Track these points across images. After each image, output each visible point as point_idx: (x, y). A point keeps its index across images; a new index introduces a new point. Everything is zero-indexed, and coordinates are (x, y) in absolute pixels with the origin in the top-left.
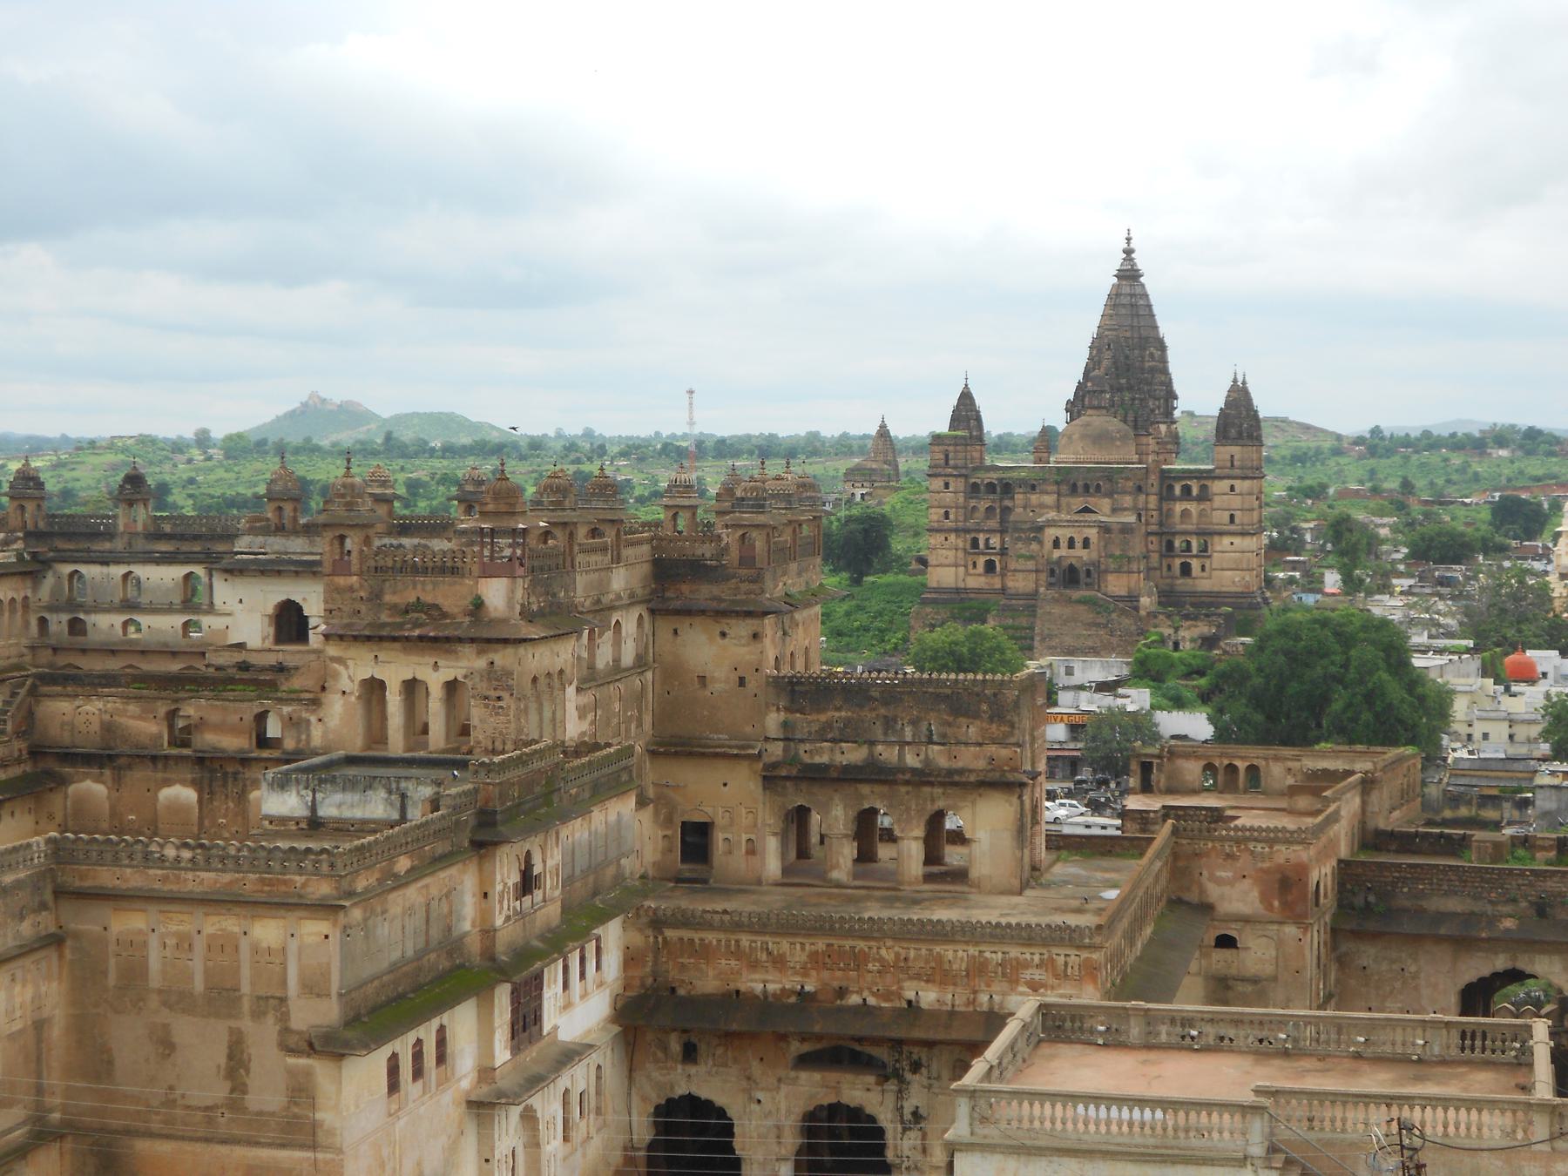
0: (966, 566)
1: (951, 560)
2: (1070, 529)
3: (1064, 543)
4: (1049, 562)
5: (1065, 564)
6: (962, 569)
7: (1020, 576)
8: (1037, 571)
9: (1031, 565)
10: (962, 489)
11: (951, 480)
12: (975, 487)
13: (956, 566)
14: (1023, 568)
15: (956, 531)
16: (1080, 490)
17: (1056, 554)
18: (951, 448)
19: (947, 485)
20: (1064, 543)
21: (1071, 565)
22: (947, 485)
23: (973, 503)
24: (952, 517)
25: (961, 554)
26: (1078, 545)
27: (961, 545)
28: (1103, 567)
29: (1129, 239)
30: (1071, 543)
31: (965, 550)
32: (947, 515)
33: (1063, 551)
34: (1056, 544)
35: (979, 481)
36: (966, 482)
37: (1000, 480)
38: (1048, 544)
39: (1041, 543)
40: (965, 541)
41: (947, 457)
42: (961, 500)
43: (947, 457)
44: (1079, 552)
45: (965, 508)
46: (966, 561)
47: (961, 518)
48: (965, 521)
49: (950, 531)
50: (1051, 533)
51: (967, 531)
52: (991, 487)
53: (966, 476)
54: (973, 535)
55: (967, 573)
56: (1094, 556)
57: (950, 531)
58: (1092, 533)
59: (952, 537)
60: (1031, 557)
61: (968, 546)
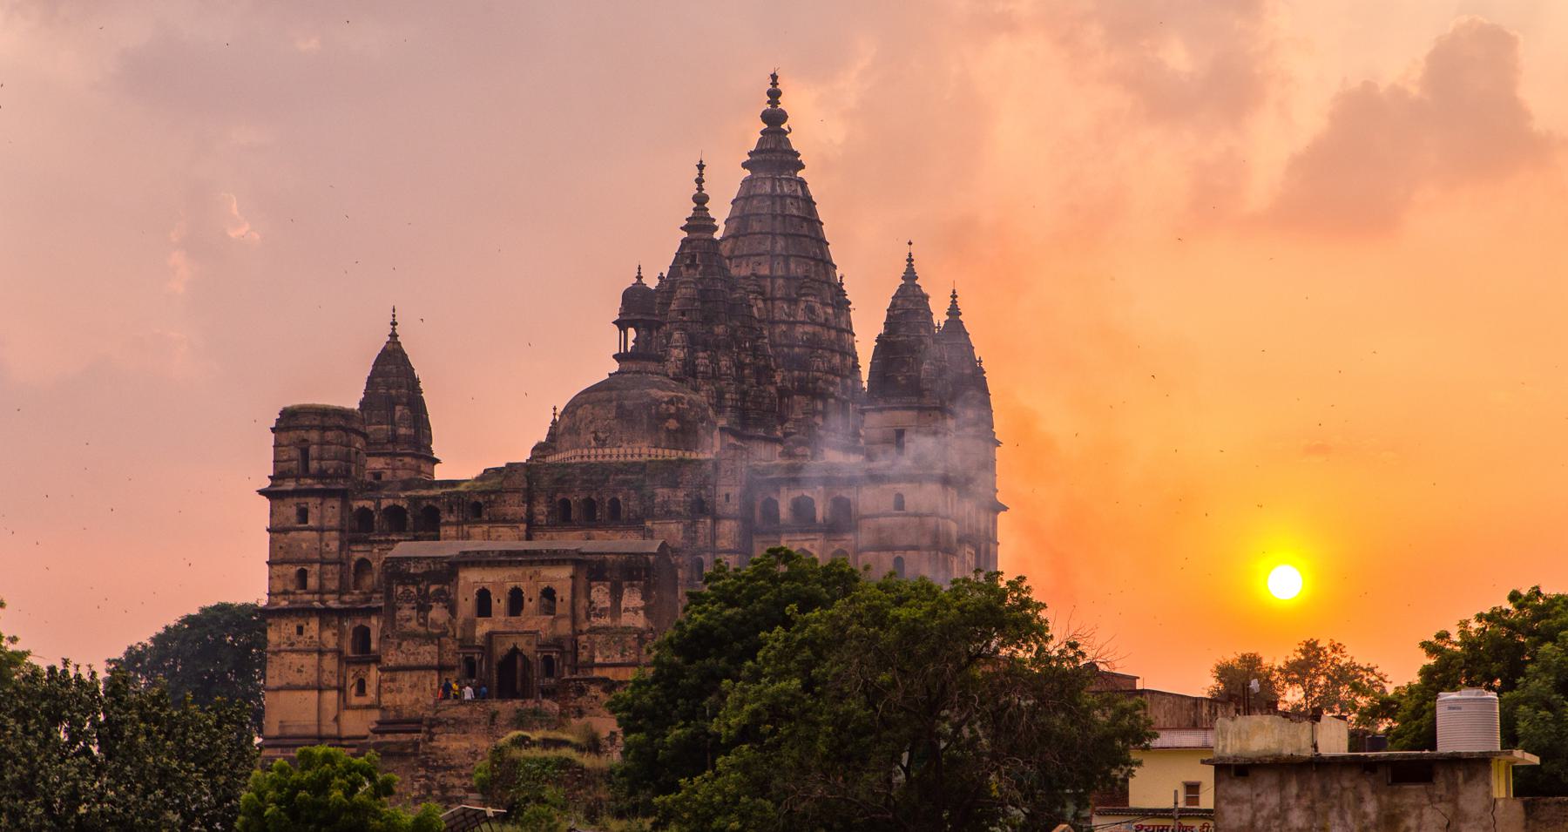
0: (341, 689)
1: (310, 675)
2: (517, 572)
3: (499, 604)
4: (466, 643)
5: (501, 649)
6: (331, 696)
7: (406, 679)
8: (441, 668)
9: (428, 653)
10: (334, 522)
11: (312, 502)
12: (364, 514)
13: (320, 689)
14: (412, 661)
15: (325, 614)
16: (574, 515)
17: (483, 628)
18: (314, 436)
19: (303, 515)
20: (499, 604)
21: (515, 651)
22: (303, 515)
23: (358, 552)
24: (312, 582)
25: (330, 663)
26: (529, 606)
27: (331, 642)
28: (584, 656)
29: (774, 95)
30: (516, 601)
31: (339, 652)
32: (302, 576)
33: (499, 619)
34: (484, 603)
35: (369, 504)
36: (345, 505)
37: (415, 501)
38: (466, 606)
39: (452, 608)
40: (341, 634)
41: (305, 453)
42: (334, 546)
43: (305, 453)
44: (533, 620)
45: (340, 562)
46: (341, 676)
47: (333, 585)
48: (341, 591)
49: (306, 612)
50: (472, 579)
51: (342, 613)
52: (395, 517)
53: (343, 495)
54: (359, 622)
55: (345, 705)
56: (564, 628)
57: (306, 612)
58: (560, 577)
59: (313, 626)
60: (429, 638)
61: (348, 650)
